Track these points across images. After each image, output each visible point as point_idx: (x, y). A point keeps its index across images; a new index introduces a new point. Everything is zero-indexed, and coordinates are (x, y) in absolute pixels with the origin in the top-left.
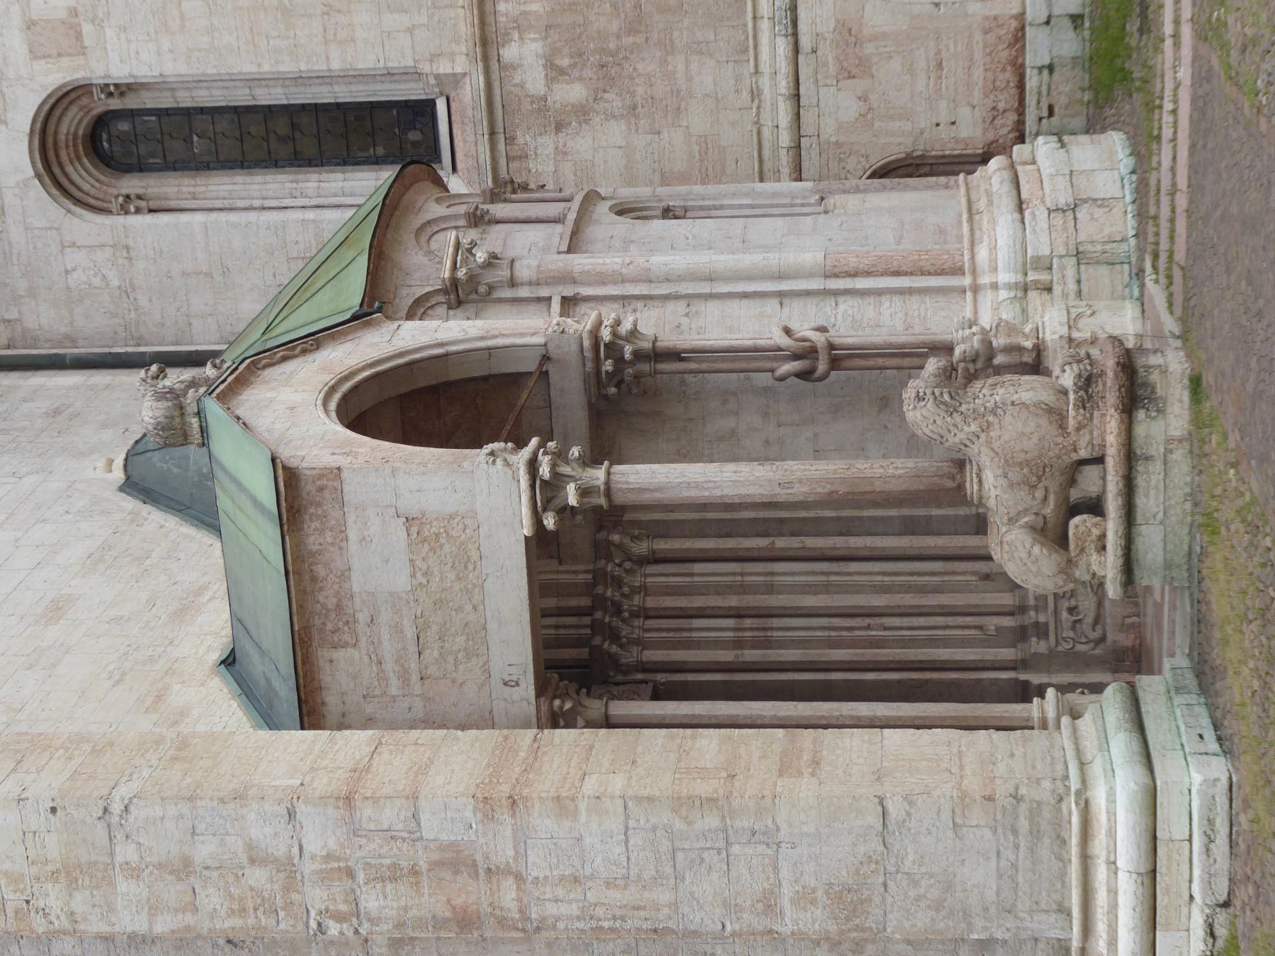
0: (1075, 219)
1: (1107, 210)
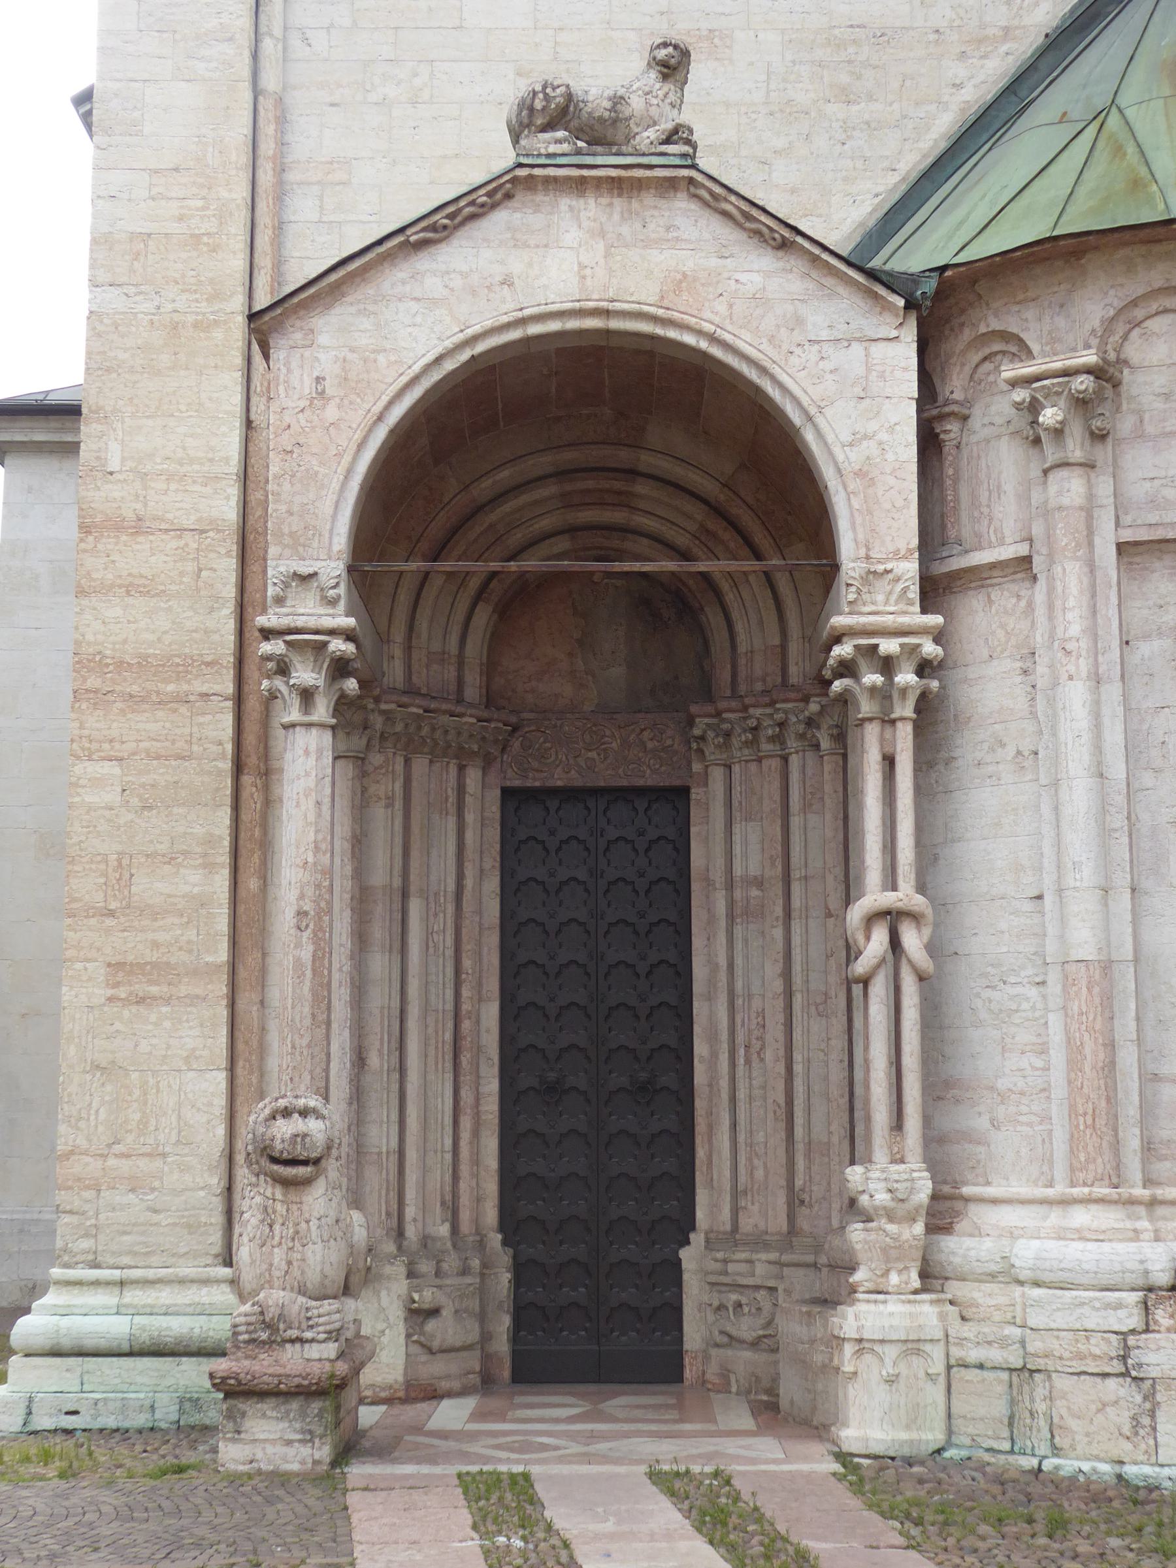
0: (1105, 1375)
1: (1127, 1430)
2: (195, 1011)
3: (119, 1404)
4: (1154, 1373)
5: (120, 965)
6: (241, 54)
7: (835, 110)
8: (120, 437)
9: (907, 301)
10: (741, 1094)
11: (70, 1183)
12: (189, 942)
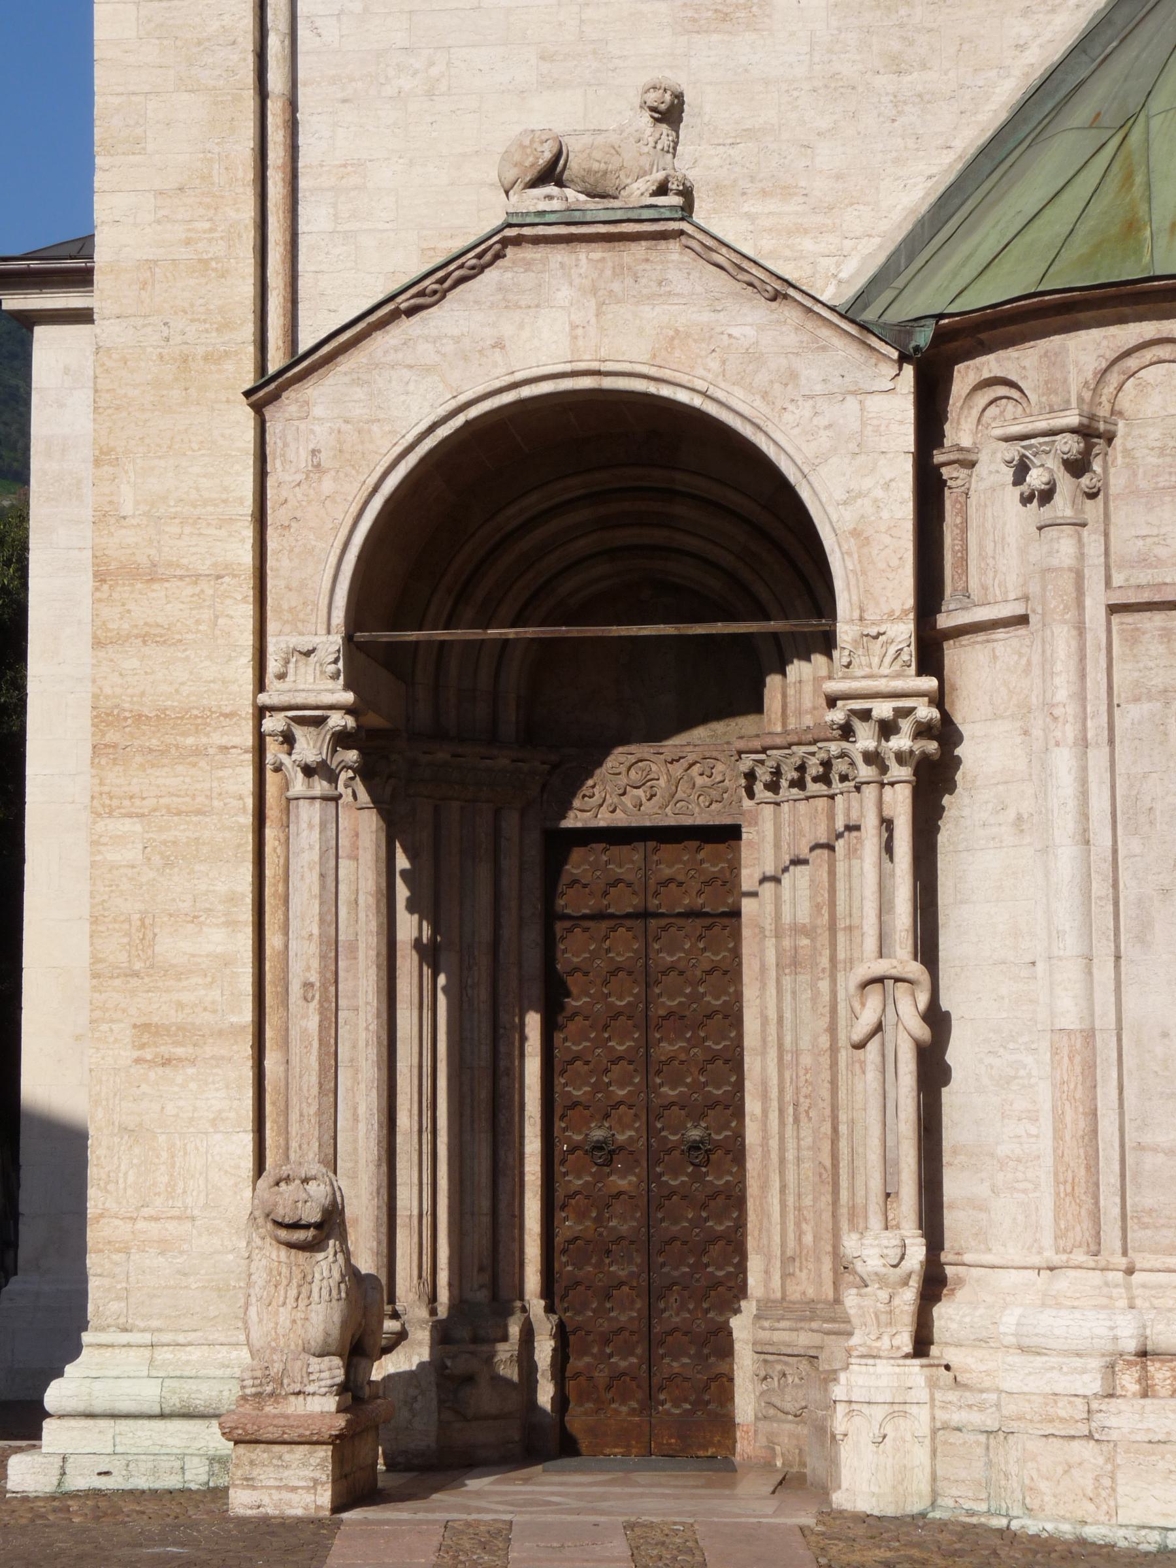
2: (220, 1072)
3: (150, 1465)
4: (1114, 1435)
5: (146, 1026)
6: (245, 60)
7: (883, 81)
8: (132, 480)
9: (901, 353)
10: (790, 1155)
11: (101, 1246)
12: (213, 1002)
